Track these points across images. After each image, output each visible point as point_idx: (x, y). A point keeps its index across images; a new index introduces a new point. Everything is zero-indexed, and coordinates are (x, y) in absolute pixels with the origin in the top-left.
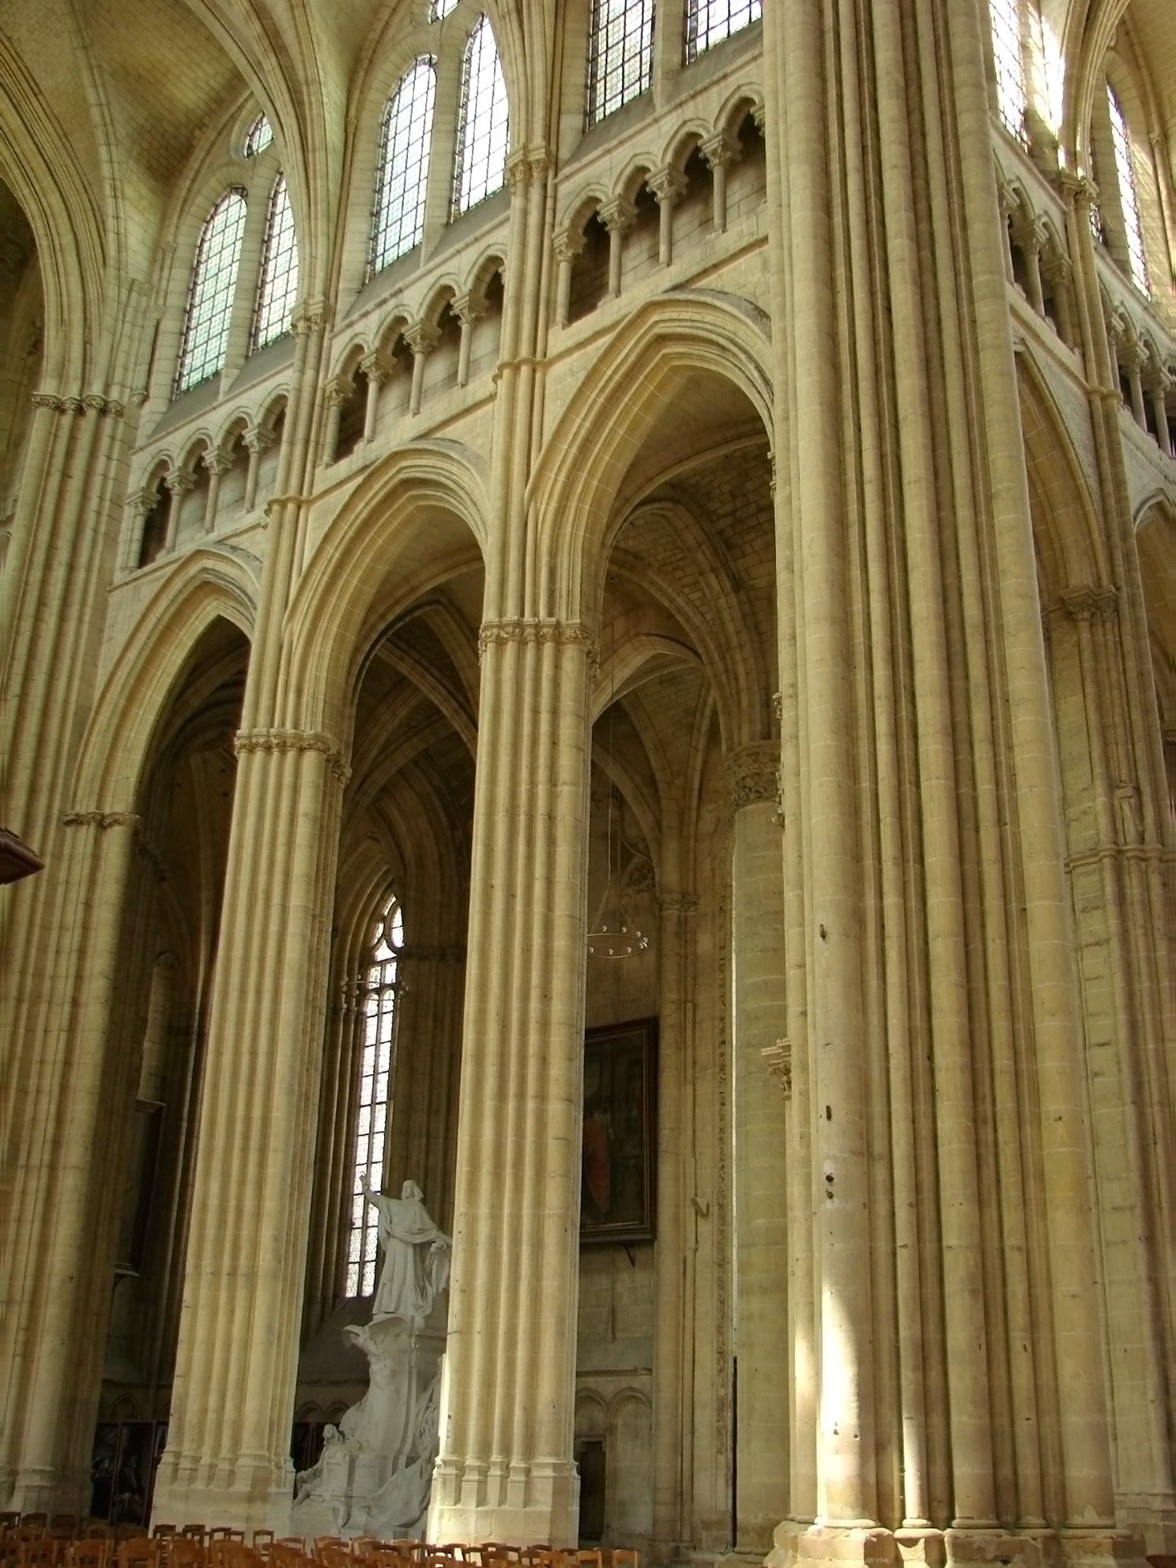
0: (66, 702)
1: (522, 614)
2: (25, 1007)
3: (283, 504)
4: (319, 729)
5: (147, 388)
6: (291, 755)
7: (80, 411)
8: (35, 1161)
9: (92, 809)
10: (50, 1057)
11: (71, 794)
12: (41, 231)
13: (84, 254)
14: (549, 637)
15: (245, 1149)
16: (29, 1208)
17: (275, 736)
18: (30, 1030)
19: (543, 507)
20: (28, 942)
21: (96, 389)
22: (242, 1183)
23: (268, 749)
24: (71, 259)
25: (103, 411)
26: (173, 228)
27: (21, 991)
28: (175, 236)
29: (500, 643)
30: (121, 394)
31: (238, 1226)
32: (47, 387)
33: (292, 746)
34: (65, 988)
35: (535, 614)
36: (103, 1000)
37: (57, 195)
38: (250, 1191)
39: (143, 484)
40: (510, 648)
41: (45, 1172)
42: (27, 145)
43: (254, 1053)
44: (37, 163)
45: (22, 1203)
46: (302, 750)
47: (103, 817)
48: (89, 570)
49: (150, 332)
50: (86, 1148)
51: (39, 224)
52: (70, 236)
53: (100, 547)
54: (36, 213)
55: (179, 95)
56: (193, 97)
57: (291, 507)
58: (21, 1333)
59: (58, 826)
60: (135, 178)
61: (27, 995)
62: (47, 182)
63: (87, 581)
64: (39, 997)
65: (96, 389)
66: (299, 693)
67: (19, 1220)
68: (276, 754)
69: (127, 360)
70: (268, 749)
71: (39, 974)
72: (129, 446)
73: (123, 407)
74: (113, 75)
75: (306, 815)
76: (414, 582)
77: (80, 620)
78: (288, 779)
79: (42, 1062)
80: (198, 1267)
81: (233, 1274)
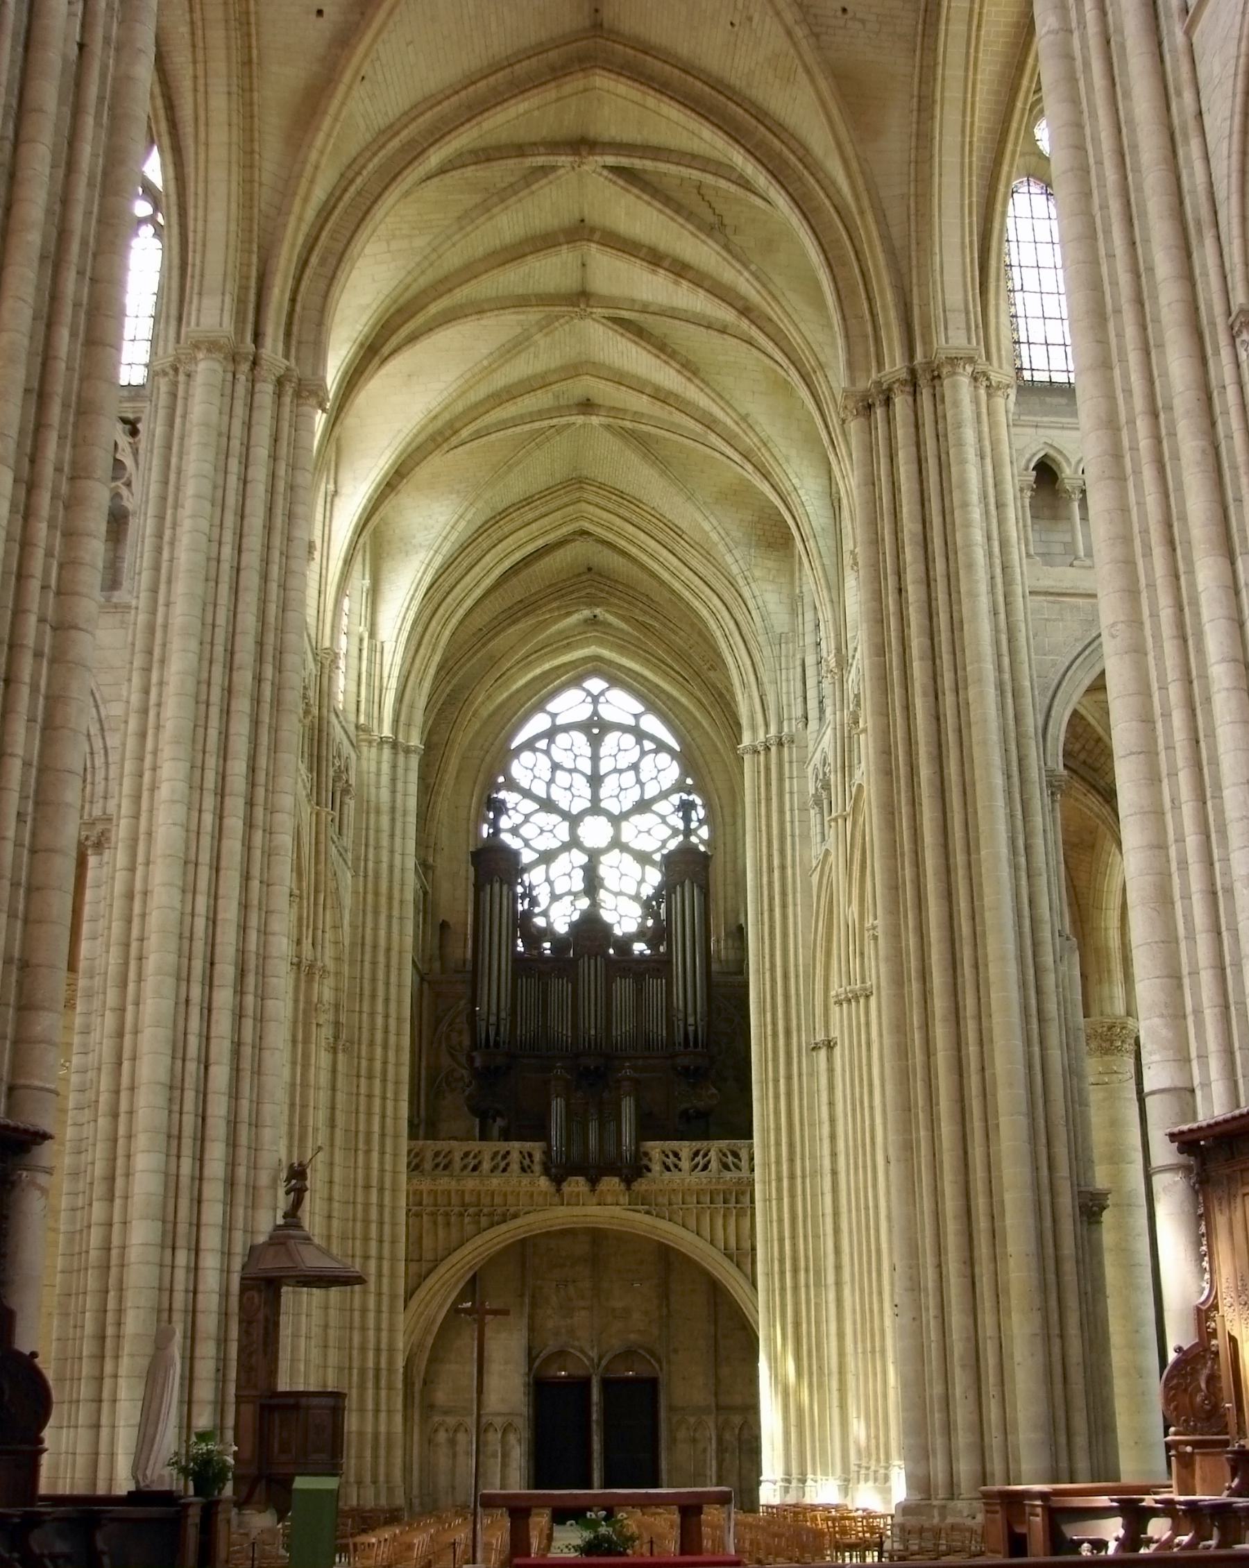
0: (796, 966)
3: (836, 820)
6: (862, 1001)
7: (768, 749)
9: (823, 1038)
20: (802, 1137)
21: (773, 730)
22: (871, 1294)
23: (849, 1001)
25: (780, 744)
30: (790, 726)
31: (872, 1321)
32: (747, 739)
48: (793, 867)
49: (799, 669)
53: (797, 847)
57: (840, 821)
60: (759, 560)
63: (794, 874)
65: (773, 730)
69: (789, 700)
70: (849, 1001)
72: (803, 762)
77: (795, 905)
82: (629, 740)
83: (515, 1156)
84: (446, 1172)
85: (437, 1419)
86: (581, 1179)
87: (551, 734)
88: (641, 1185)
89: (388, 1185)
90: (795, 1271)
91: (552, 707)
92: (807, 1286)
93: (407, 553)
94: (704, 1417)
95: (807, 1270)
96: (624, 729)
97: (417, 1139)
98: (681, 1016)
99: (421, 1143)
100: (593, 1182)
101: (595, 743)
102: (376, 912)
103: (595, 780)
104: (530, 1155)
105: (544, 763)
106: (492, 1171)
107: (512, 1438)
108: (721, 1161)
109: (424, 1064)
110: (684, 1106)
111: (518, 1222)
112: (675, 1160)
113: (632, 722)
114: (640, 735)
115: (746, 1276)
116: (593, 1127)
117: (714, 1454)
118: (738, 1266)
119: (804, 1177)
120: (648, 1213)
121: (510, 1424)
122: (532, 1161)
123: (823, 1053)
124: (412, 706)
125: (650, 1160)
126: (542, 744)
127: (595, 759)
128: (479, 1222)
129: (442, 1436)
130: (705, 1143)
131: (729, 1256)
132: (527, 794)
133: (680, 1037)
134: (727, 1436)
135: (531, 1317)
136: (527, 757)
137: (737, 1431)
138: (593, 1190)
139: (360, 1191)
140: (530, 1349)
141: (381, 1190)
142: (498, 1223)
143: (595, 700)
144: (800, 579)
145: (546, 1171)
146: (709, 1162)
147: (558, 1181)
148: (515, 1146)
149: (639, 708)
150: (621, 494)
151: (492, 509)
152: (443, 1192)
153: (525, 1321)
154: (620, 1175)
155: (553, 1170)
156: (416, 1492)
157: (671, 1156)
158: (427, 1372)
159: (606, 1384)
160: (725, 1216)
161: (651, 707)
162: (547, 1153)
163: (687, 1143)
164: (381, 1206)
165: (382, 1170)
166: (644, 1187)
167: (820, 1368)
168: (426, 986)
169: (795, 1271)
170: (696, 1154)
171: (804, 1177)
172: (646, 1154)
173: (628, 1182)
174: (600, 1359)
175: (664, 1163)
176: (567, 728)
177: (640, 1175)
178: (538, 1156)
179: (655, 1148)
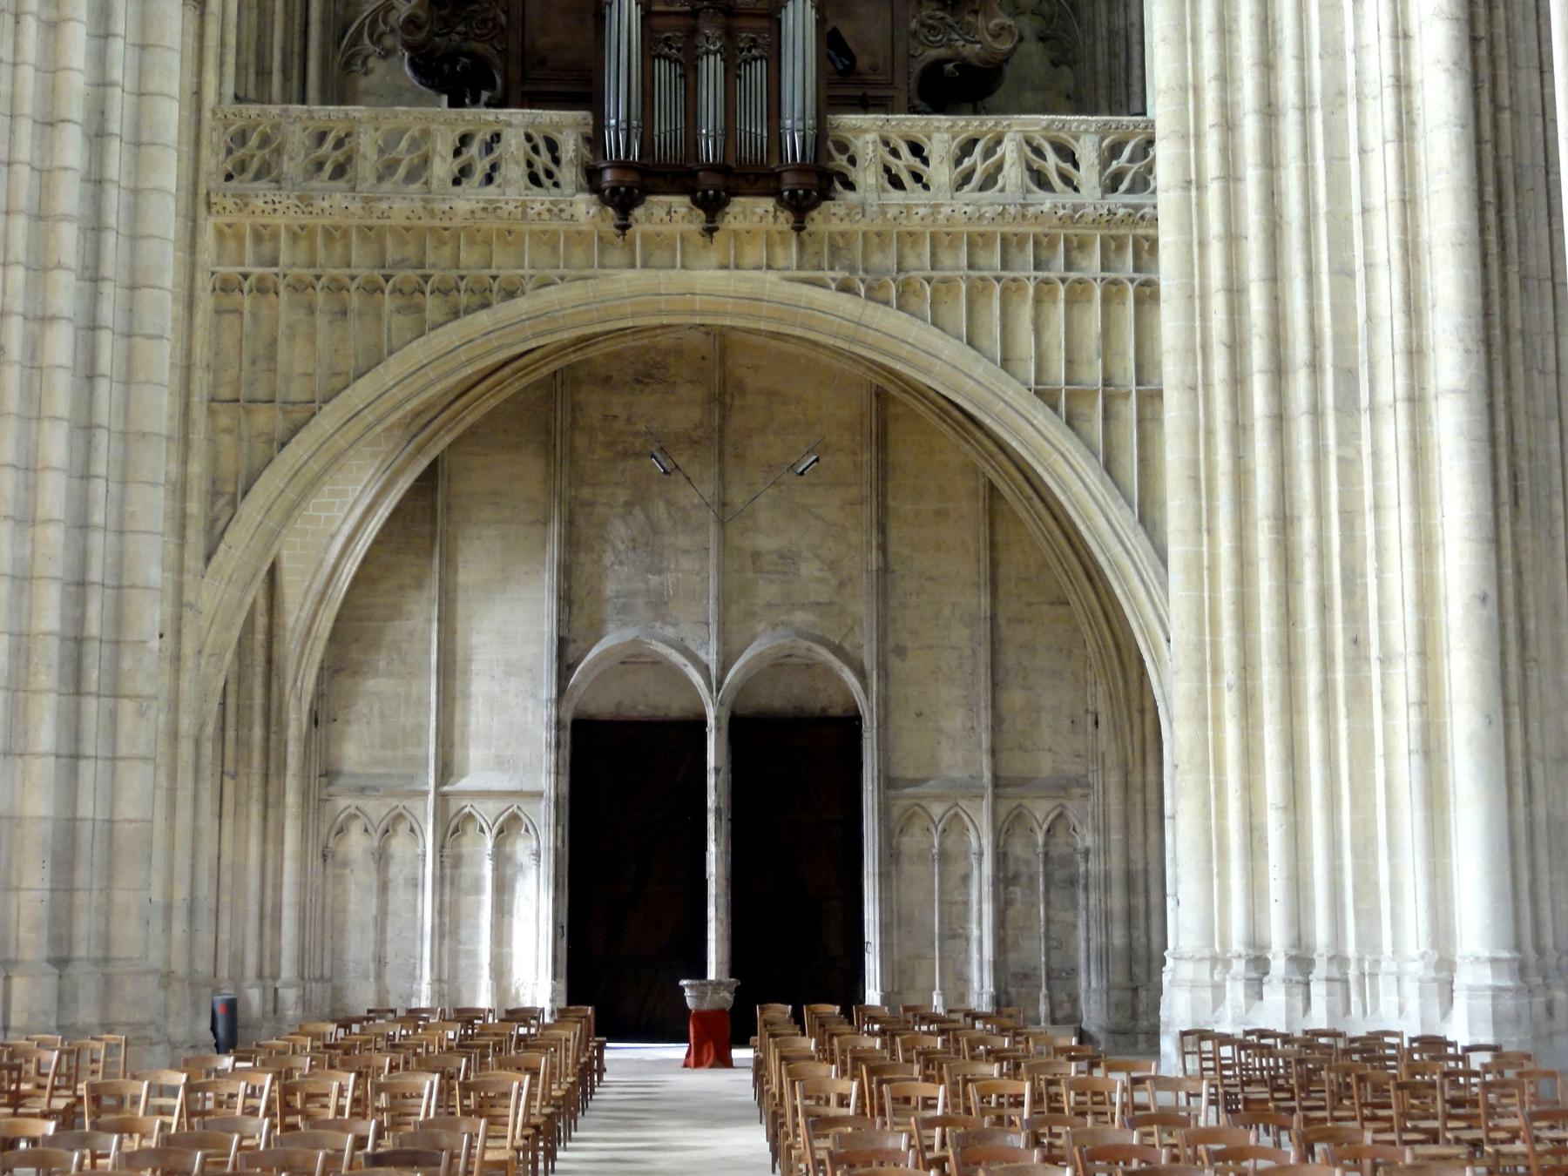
2: (1318, 118)
8: (1385, 394)
10: (1377, 199)
16: (1390, 483)
18: (1335, 159)
27: (1304, 89)
34: (1379, 64)
36: (1448, 63)
41: (1402, 407)
45: (1377, 476)
50: (1467, 351)
58: (1414, 711)
61: (1317, 96)
64: (1342, 93)
67: (1377, 508)
71: (1333, 51)
79: (1365, 210)
83: (513, 144)
84: (341, 184)
85: (343, 803)
86: (681, 203)
88: (829, 219)
89: (118, 119)
90: (1279, 370)
92: (1316, 412)
94: (963, 803)
95: (1315, 367)
97: (263, 98)
99: (275, 109)
100: (712, 207)
104: (552, 146)
106: (456, 182)
107: (522, 849)
108: (1030, 168)
110: (934, 53)
111: (521, 305)
112: (916, 163)
115: (1090, 446)
116: (712, 69)
117: (987, 889)
118: (1070, 422)
119: (1305, 109)
120: (845, 288)
121: (515, 818)
122: (556, 161)
125: (852, 161)
128: (420, 309)
129: (357, 844)
130: (990, 121)
131: (1046, 396)
134: (1018, 848)
135: (566, 572)
137: (1040, 839)
138: (710, 231)
139: (25, 128)
140: (562, 644)
141: (97, 136)
142: (469, 310)
145: (592, 177)
146: (999, 167)
147: (623, 202)
148: (516, 122)
152: (328, 233)
153: (547, 581)
154: (776, 193)
155: (608, 176)
156: (288, 971)
157: (904, 150)
158: (319, 696)
159: (741, 728)
160: (1038, 301)
162: (595, 140)
163: (943, 120)
164: (96, 181)
165: (102, 84)
166: (836, 226)
169: (1279, 370)
170: (968, 147)
171: (1305, 109)
172: (843, 147)
173: (800, 207)
174: (724, 668)
175: (887, 170)
177: (826, 195)
178: (569, 146)
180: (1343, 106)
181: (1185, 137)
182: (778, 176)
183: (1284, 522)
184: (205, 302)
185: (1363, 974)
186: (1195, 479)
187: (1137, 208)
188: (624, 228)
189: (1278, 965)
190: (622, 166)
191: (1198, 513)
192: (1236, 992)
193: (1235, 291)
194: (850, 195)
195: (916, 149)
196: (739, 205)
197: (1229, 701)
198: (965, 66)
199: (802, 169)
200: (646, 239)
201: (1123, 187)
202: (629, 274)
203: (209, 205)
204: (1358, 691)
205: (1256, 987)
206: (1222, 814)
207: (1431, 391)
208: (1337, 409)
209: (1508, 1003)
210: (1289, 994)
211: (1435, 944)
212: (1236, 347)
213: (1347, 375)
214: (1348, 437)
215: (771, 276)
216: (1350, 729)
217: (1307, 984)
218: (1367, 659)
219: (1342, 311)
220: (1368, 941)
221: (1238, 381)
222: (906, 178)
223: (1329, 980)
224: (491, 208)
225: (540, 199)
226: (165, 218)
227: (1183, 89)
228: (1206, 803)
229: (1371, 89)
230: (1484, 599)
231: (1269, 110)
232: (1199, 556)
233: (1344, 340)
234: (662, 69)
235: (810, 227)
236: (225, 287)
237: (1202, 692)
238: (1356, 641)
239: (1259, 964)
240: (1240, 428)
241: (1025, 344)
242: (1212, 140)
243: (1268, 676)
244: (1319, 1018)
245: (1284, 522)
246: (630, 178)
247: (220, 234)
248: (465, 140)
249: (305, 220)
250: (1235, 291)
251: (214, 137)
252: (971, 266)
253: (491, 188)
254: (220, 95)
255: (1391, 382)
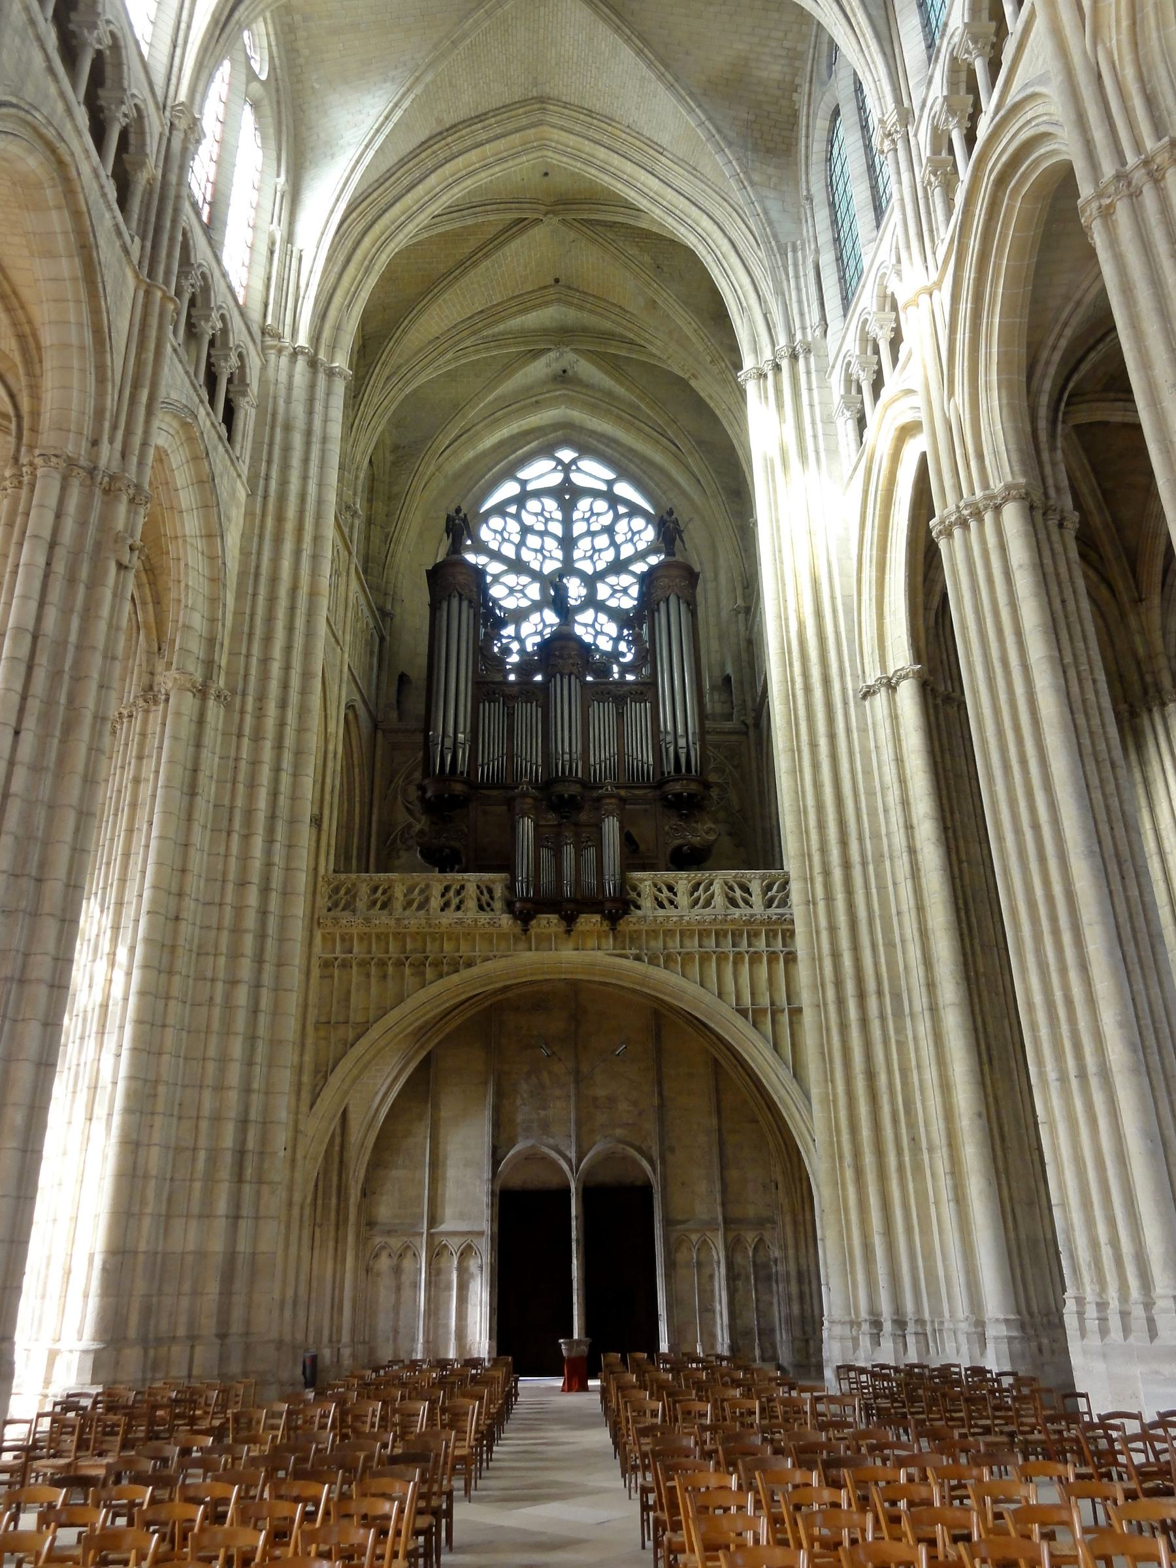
0: (833, 598)
1: (1124, 163)
2: (871, 868)
4: (1009, 478)
5: (823, 317)
6: (988, 517)
7: (777, 368)
8: (918, 1007)
10: (905, 908)
11: (860, 672)
12: (704, 253)
13: (741, 248)
14: (1166, 164)
15: (1056, 932)
17: (966, 507)
18: (882, 888)
19: (1114, 42)
22: (1063, 971)
24: (734, 259)
25: (794, 357)
26: (804, 185)
28: (808, 190)
29: (1107, 213)
32: (748, 362)
33: (986, 508)
34: (899, 840)
35: (1138, 146)
36: (933, 839)
37: (705, 216)
38: (1074, 976)
39: (842, 392)
40: (1122, 215)
41: (927, 1014)
42: (670, 194)
43: (1036, 827)
44: (682, 203)
45: (917, 1050)
46: (997, 509)
47: (889, 679)
50: (957, 983)
51: (701, 248)
52: (726, 241)
54: (695, 241)
55: (765, 74)
56: (778, 68)
58: (948, 1177)
59: (856, 703)
60: (758, 164)
61: (870, 858)
62: (695, 212)
64: (882, 856)
66: (980, 456)
67: (919, 1067)
68: (973, 525)
70: (964, 524)
71: (875, 835)
73: (809, 344)
74: (705, 94)
75: (1021, 566)
76: (1078, 295)
78: (992, 541)
79: (899, 913)
80: (1042, 1074)
81: (1083, 1075)
82: (601, 505)
83: (471, 890)
84: (385, 912)
85: (378, 1240)
86: (554, 918)
87: (521, 500)
88: (628, 924)
89: (276, 882)
90: (861, 996)
91: (522, 475)
92: (882, 1017)
93: (333, 156)
94: (708, 1234)
95: (880, 993)
96: (595, 494)
97: (348, 870)
98: (670, 738)
99: (353, 876)
100: (569, 920)
101: (567, 508)
102: (278, 540)
103: (568, 542)
104: (490, 891)
105: (513, 526)
106: (442, 910)
107: (473, 1264)
108: (727, 896)
109: (375, 818)
110: (677, 842)
111: (475, 971)
112: (671, 895)
113: (604, 487)
114: (613, 500)
115: (765, 1037)
117: (724, 1283)
118: (755, 1025)
119: (864, 864)
120: (638, 958)
121: (469, 1247)
122: (492, 898)
123: (881, 699)
124: (338, 328)
125: (639, 895)
126: (512, 509)
127: (567, 522)
128: (423, 974)
129: (384, 1263)
130: (707, 874)
131: (743, 1012)
132: (496, 556)
133: (669, 767)
134: (739, 1259)
135: (497, 1110)
136: (496, 522)
137: (751, 1254)
138: (568, 932)
139: (230, 887)
140: (495, 1149)
141: (265, 890)
142: (448, 974)
143: (566, 468)
144: (807, 182)
145: (509, 906)
146: (712, 896)
148: (472, 879)
149: (610, 475)
150: (590, 113)
151: (439, 121)
152: (378, 936)
153: (488, 1114)
154: (601, 912)
155: (518, 905)
156: (346, 1338)
157: (665, 890)
158: (367, 1179)
159: (589, 1193)
160: (735, 963)
161: (623, 473)
162: (511, 887)
164: (263, 912)
165: (268, 865)
166: (632, 927)
167: (914, 1140)
168: (380, 734)
169: (861, 996)
170: (696, 887)
171: (864, 864)
172: (634, 888)
174: (579, 1160)
175: (656, 899)
176: (538, 494)
177: (627, 912)
178: (498, 891)
179: (645, 881)
180: (883, 862)
181: (805, 879)
182: (602, 903)
183: (871, 1076)
184: (316, 972)
185: (934, 1330)
186: (823, 1054)
187: (782, 915)
188: (525, 931)
189: (888, 1326)
190: (524, 900)
191: (825, 1072)
192: (865, 1342)
193: (836, 955)
194: (639, 913)
195: (671, 889)
196: (583, 918)
197: (849, 1174)
198: (693, 848)
199: (613, 900)
200: (538, 936)
201: (774, 905)
202: (528, 954)
203: (319, 924)
204: (918, 1168)
205: (876, 1339)
206: (849, 1238)
207: (941, 1006)
208: (894, 1015)
209: (1017, 1346)
210: (895, 1343)
211: (972, 1312)
212: (839, 984)
213: (897, 997)
214: (900, 1030)
215: (599, 953)
216: (914, 1187)
217: (904, 1337)
218: (921, 1149)
219: (891, 964)
220: (936, 1311)
221: (841, 1002)
222: (666, 903)
223: (916, 1334)
224: (460, 922)
225: (484, 917)
226: (298, 930)
227: (803, 855)
228: (841, 1232)
229: (897, 853)
230: (980, 1115)
231: (846, 865)
232: (827, 1094)
233: (894, 978)
234: (544, 853)
235: (619, 928)
236: (326, 964)
237: (834, 1169)
238: (913, 1139)
239: (877, 1324)
240: (844, 1027)
241: (730, 987)
242: (819, 880)
243: (868, 1159)
244: (913, 1357)
245: (871, 1076)
246: (529, 905)
247: (324, 937)
248: (447, 889)
249: (366, 930)
250: (836, 955)
251: (323, 889)
252: (700, 946)
253: (460, 912)
254: (326, 870)
255: (920, 1001)
